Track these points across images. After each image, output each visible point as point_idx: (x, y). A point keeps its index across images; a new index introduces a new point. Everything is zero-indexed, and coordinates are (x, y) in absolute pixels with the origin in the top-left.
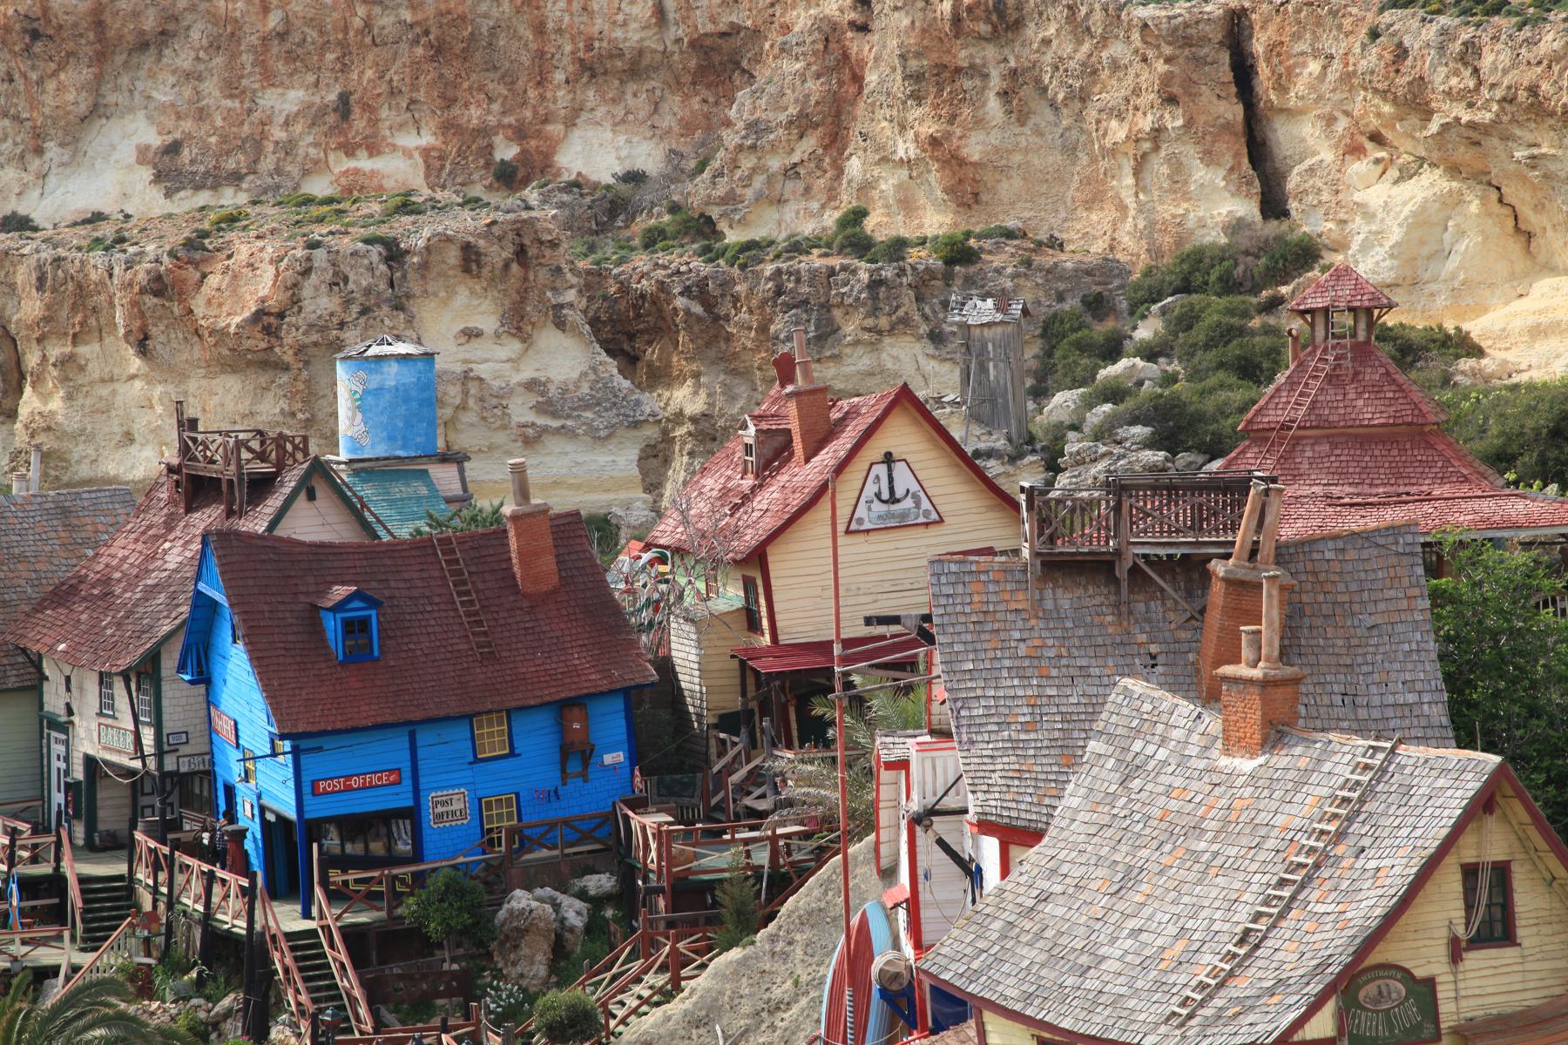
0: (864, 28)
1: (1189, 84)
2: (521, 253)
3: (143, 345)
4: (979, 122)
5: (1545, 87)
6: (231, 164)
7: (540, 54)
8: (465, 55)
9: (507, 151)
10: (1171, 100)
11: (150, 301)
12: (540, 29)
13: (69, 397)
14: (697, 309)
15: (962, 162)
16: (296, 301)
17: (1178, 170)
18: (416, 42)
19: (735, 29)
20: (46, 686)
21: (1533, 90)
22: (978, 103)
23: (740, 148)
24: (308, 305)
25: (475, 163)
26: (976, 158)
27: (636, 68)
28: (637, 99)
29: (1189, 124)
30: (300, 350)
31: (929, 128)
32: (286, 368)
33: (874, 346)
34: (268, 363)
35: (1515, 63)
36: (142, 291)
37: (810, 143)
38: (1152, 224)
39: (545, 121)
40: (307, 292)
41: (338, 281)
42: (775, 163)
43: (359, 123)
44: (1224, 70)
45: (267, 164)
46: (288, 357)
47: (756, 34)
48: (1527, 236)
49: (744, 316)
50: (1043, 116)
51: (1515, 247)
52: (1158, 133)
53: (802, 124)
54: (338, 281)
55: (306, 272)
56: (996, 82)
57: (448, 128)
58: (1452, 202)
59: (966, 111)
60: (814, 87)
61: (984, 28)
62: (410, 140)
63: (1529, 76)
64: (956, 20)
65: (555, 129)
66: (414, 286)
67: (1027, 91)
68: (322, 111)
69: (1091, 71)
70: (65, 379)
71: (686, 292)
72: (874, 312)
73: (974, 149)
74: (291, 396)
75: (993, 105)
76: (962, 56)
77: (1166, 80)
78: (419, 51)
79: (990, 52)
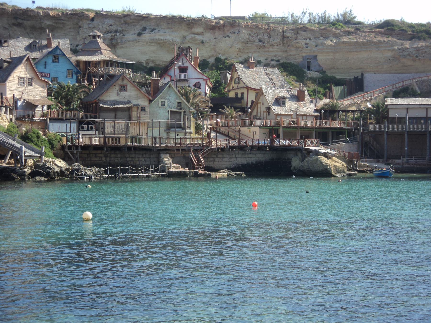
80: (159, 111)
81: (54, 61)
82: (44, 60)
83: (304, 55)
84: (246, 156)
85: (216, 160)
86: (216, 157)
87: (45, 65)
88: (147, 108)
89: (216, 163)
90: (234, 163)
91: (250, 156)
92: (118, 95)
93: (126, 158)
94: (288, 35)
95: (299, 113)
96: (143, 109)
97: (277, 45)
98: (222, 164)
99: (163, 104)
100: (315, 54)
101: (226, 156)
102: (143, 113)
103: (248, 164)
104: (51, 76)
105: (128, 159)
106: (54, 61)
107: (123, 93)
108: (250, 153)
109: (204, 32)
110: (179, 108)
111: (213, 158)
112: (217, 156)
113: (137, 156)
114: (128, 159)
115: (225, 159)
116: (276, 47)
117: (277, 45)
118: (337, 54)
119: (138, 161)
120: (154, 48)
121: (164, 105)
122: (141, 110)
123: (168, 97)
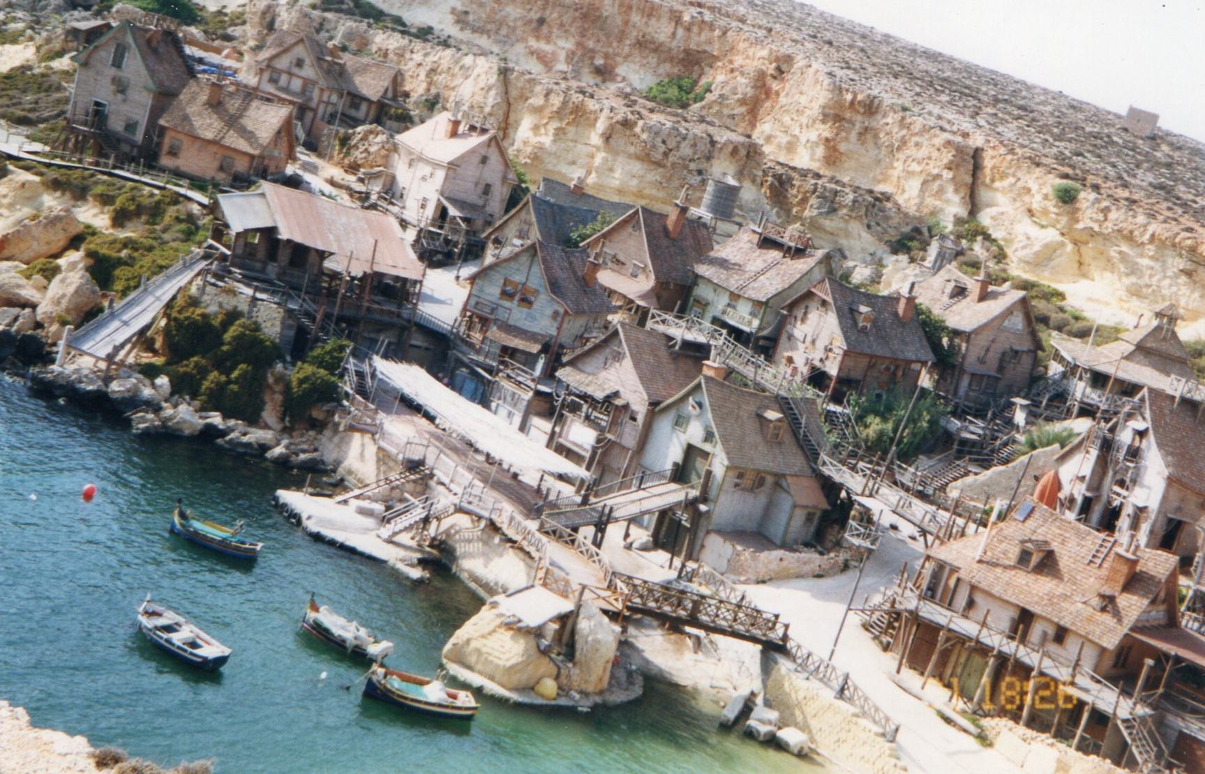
0: (775, 78)
1: (958, 166)
2: (748, 155)
3: (607, 137)
4: (847, 139)
5: (1136, 233)
6: (489, 27)
7: (623, 32)
8: (593, 22)
9: (599, 61)
10: (950, 169)
11: (618, 126)
12: (626, 23)
13: (554, 141)
14: (776, 183)
16: (678, 147)
17: (941, 191)
18: (576, 10)
19: (705, 52)
21: (1131, 232)
22: (848, 133)
23: (715, 101)
24: (682, 150)
25: (587, 62)
27: (657, 49)
28: (653, 60)
29: (953, 178)
30: (673, 164)
31: (827, 134)
32: (663, 166)
33: (847, 221)
34: (659, 164)
35: (1126, 220)
36: (617, 122)
37: (743, 109)
38: (921, 203)
39: (618, 55)
40: (683, 145)
41: (694, 145)
42: (726, 111)
43: (545, 29)
44: (971, 167)
45: (504, 31)
46: (669, 165)
47: (717, 58)
48: (1081, 264)
49: (794, 191)
51: (1076, 265)
52: (938, 176)
53: (742, 102)
54: (694, 145)
55: (684, 139)
56: (858, 125)
57: (579, 44)
58: (1063, 244)
59: (843, 134)
60: (750, 91)
61: (862, 110)
62: (561, 43)
63: (1131, 227)
64: (852, 103)
65: (619, 59)
66: (716, 154)
67: (869, 136)
68: (530, 21)
69: (904, 142)
70: (556, 135)
71: (774, 176)
72: (852, 210)
73: (842, 147)
74: (663, 177)
75: (853, 136)
76: (848, 115)
77: (951, 162)
78: (577, 14)
79: (859, 118)
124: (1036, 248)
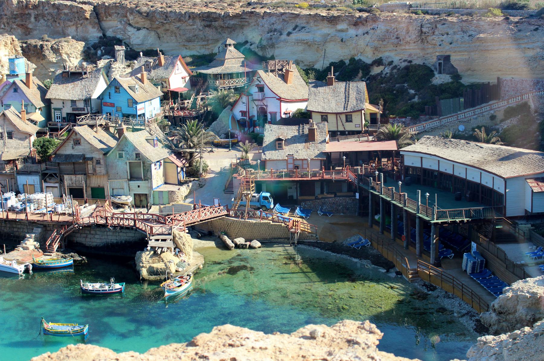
15: (27, 28)
20: (52, 104)
26: (31, 28)
48: (159, 38)
50: (42, 21)
73: (30, 26)
75: (33, 19)
80: (118, 163)
81: (116, 92)
82: (108, 91)
83: (437, 54)
84: (117, 234)
85: (89, 236)
86: (89, 233)
87: (110, 95)
88: (102, 161)
89: (88, 240)
90: (105, 240)
91: (121, 234)
92: (73, 148)
93: (14, 228)
94: (424, 30)
95: (295, 157)
96: (98, 162)
97: (414, 42)
98: (94, 241)
99: (121, 156)
100: (447, 54)
101: (98, 233)
102: (98, 166)
103: (117, 243)
104: (115, 106)
105: (15, 230)
106: (116, 92)
107: (77, 147)
108: (121, 232)
109: (349, 28)
110: (138, 159)
111: (86, 234)
112: (90, 232)
113: (22, 227)
114: (15, 230)
115: (97, 236)
116: (413, 44)
117: (414, 42)
118: (472, 54)
119: (23, 232)
120: (301, 48)
121: (122, 157)
122: (97, 163)
123: (126, 149)
124: (141, 38)
